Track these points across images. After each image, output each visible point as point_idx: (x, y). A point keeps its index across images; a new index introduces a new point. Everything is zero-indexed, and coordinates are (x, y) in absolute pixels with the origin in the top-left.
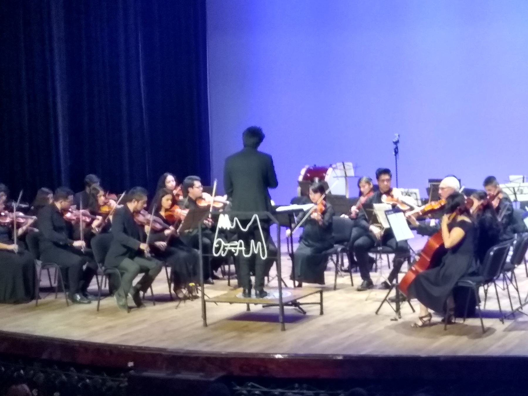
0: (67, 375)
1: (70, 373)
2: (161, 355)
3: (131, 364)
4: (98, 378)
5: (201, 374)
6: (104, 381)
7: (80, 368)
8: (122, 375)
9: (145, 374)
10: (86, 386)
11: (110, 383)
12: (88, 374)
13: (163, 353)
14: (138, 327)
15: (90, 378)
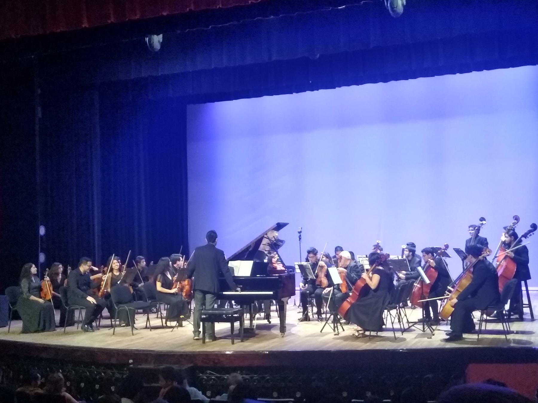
0: (89, 371)
1: (92, 369)
2: (151, 354)
3: (131, 361)
4: (109, 372)
5: (177, 365)
6: (114, 373)
7: (98, 365)
8: (125, 369)
9: (139, 366)
10: (101, 378)
11: (118, 375)
12: (104, 369)
13: (152, 353)
14: (138, 341)
15: (104, 373)
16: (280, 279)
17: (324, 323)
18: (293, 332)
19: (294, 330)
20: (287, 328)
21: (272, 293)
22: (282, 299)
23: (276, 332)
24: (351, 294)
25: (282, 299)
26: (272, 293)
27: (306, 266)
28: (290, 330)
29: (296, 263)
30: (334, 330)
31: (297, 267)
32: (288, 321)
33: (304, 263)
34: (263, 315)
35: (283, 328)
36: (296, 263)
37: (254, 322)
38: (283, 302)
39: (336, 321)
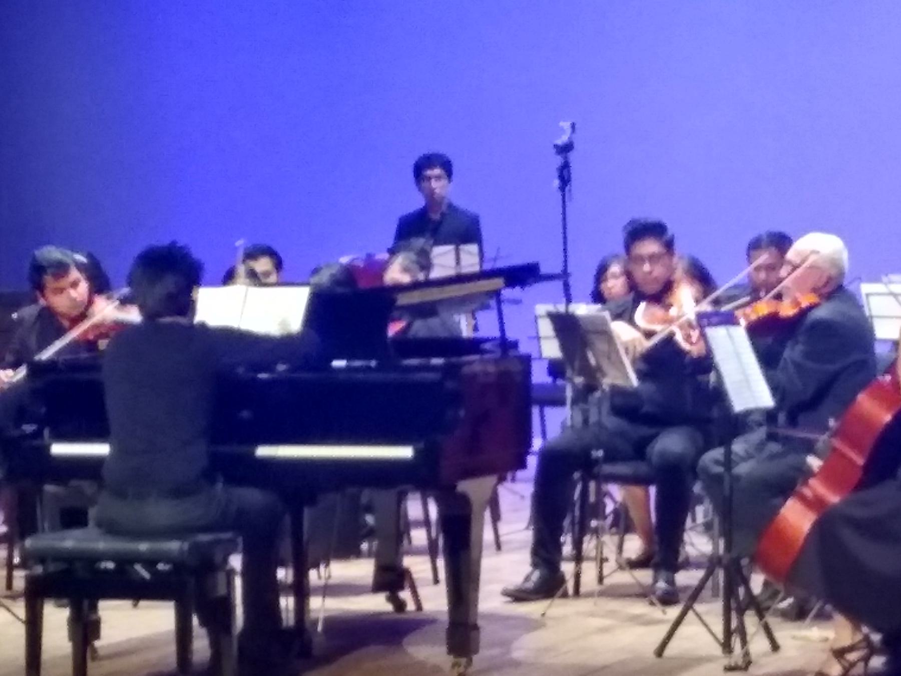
16: (450, 385)
17: (674, 612)
18: (517, 654)
19: (525, 647)
20: (487, 633)
21: (405, 452)
22: (466, 486)
23: (430, 651)
24: (814, 462)
25: (466, 486)
26: (405, 452)
27: (590, 319)
28: (506, 644)
29: (542, 309)
30: (727, 647)
31: (546, 328)
32: (490, 600)
33: (583, 309)
34: (362, 569)
35: (462, 631)
36: (542, 309)
37: (315, 603)
38: (464, 501)
39: (737, 603)
